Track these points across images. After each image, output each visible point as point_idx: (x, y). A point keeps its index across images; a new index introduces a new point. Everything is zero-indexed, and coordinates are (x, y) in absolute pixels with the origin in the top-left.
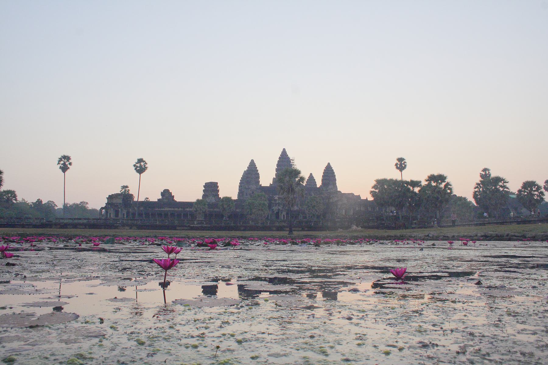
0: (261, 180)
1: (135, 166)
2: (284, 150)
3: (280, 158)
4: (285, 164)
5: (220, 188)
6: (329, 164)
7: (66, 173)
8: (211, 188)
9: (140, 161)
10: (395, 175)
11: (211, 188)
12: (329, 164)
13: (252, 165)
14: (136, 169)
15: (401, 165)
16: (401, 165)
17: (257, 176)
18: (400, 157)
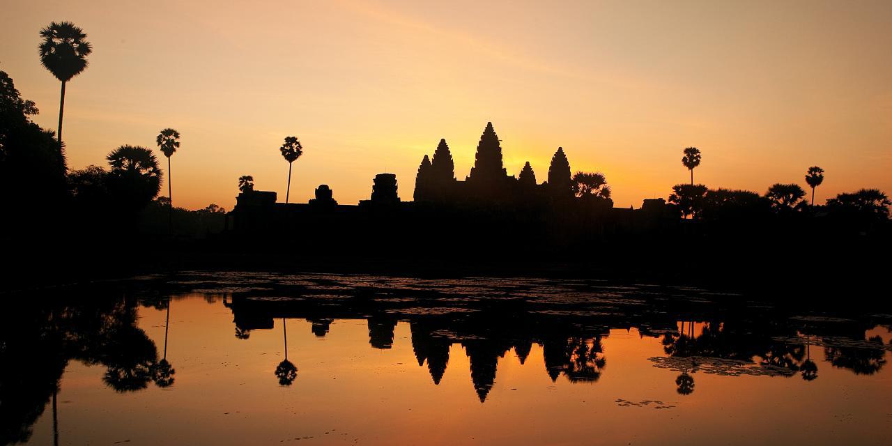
0: (455, 170)
1: (282, 149)
2: (490, 124)
3: (482, 137)
4: (489, 146)
5: (398, 184)
6: (560, 149)
7: (171, 157)
8: (385, 184)
9: (291, 140)
10: (684, 177)
11: (385, 184)
12: (560, 149)
13: (443, 146)
14: (284, 154)
15: (692, 157)
16: (692, 158)
17: (450, 165)
18: (689, 147)
